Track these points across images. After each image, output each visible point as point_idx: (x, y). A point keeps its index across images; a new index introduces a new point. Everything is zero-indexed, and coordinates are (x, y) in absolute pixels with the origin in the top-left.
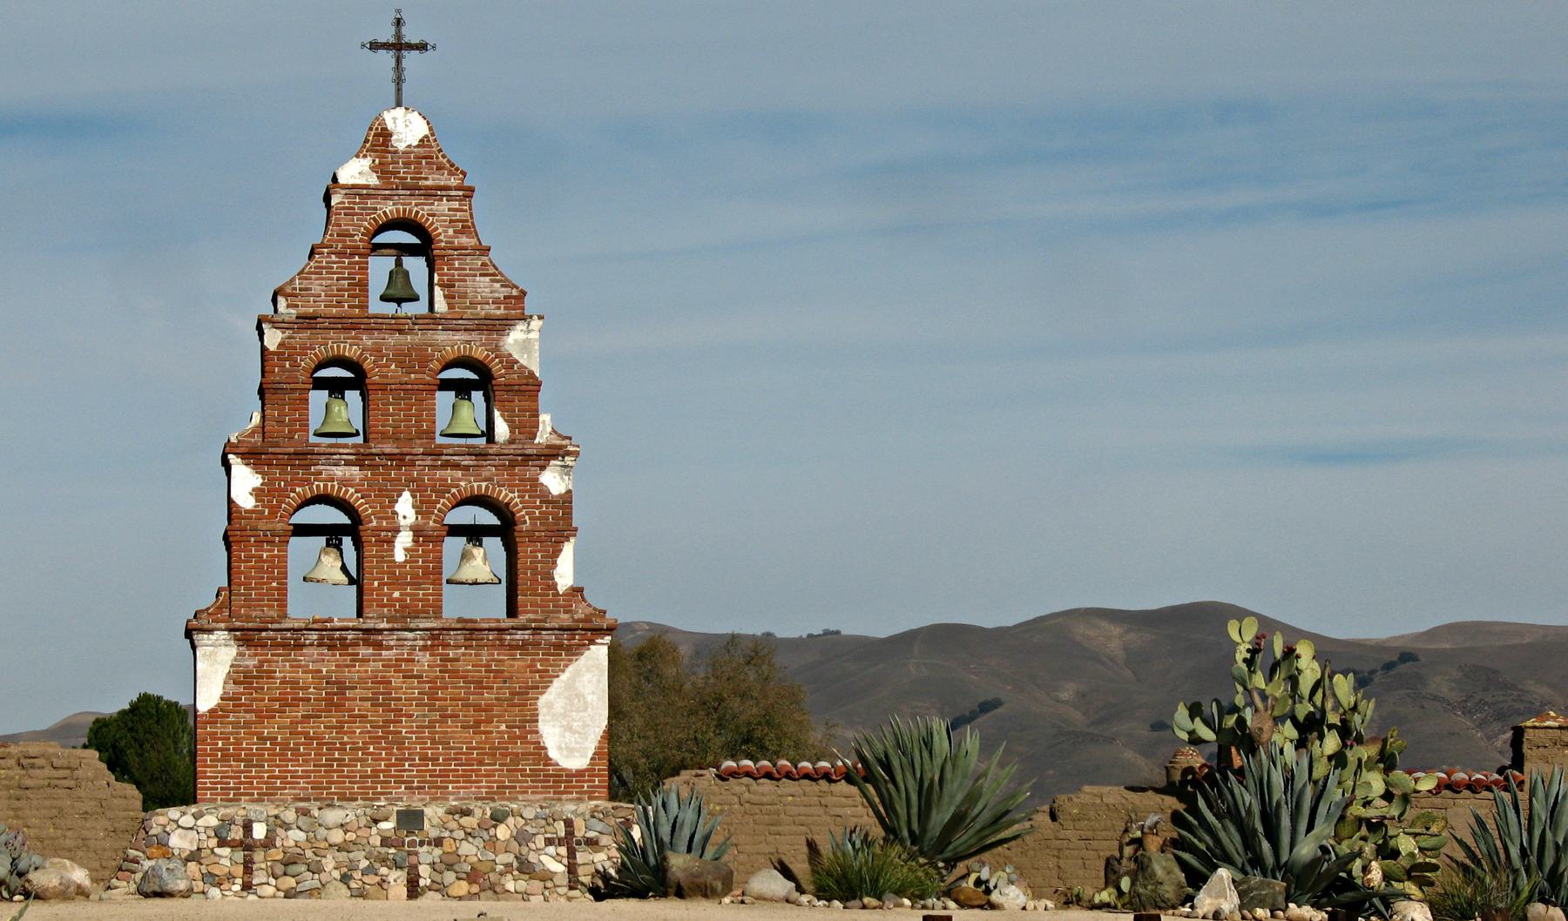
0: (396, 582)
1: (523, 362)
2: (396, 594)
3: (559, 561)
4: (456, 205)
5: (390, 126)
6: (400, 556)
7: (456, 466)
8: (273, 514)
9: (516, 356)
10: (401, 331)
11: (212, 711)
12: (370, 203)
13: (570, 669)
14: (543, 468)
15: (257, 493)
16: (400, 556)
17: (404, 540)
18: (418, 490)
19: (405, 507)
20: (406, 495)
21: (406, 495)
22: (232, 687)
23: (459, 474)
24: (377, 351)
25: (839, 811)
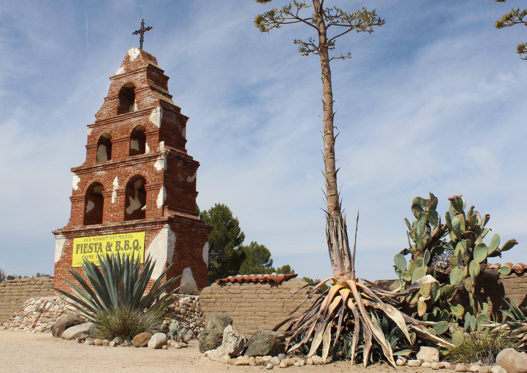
0: (112, 211)
1: (155, 124)
2: (112, 216)
3: (159, 196)
4: (142, 74)
5: (130, 54)
6: (113, 201)
7: (131, 165)
8: (83, 191)
9: (153, 122)
10: (121, 121)
11: (58, 262)
12: (120, 80)
13: (155, 239)
14: (155, 161)
15: (79, 184)
16: (113, 201)
17: (114, 194)
18: (120, 176)
19: (116, 183)
20: (116, 179)
21: (116, 179)
22: (63, 253)
23: (130, 168)
24: (116, 128)
25: (262, 296)
